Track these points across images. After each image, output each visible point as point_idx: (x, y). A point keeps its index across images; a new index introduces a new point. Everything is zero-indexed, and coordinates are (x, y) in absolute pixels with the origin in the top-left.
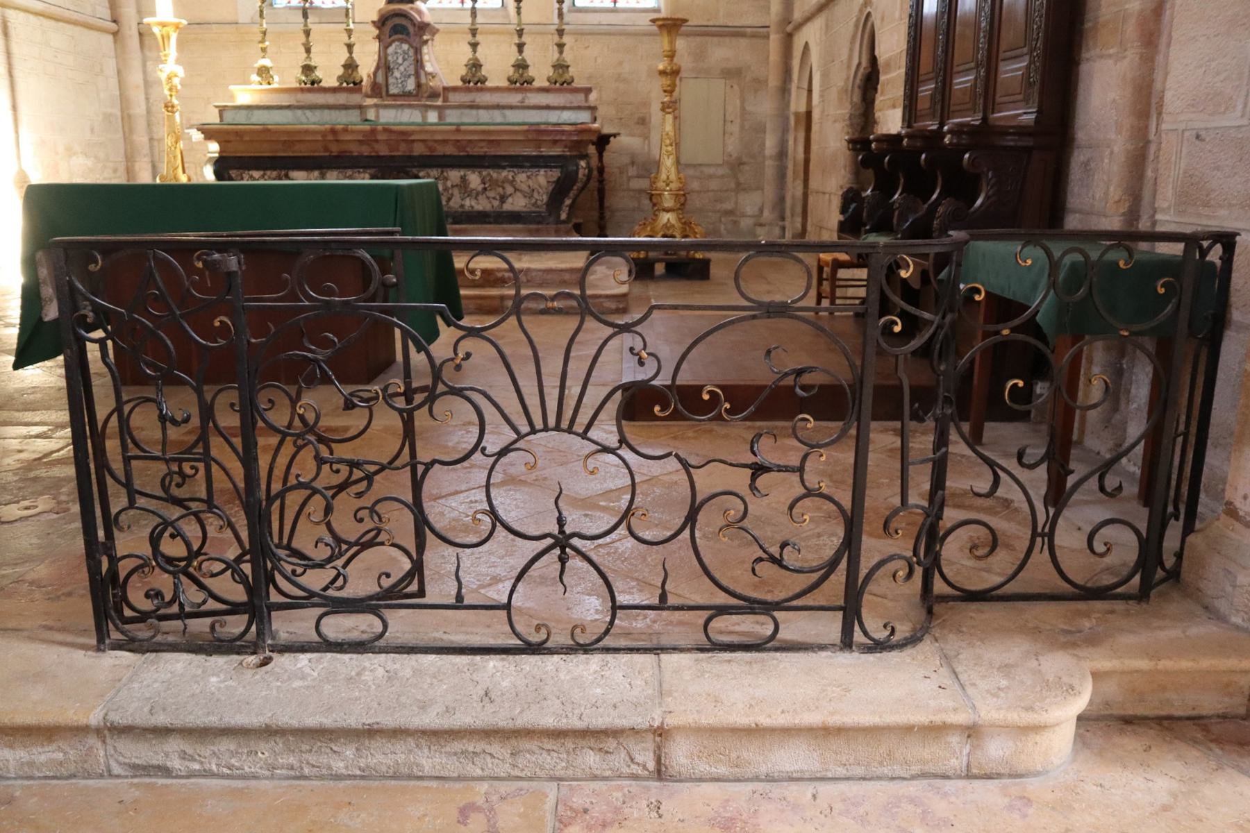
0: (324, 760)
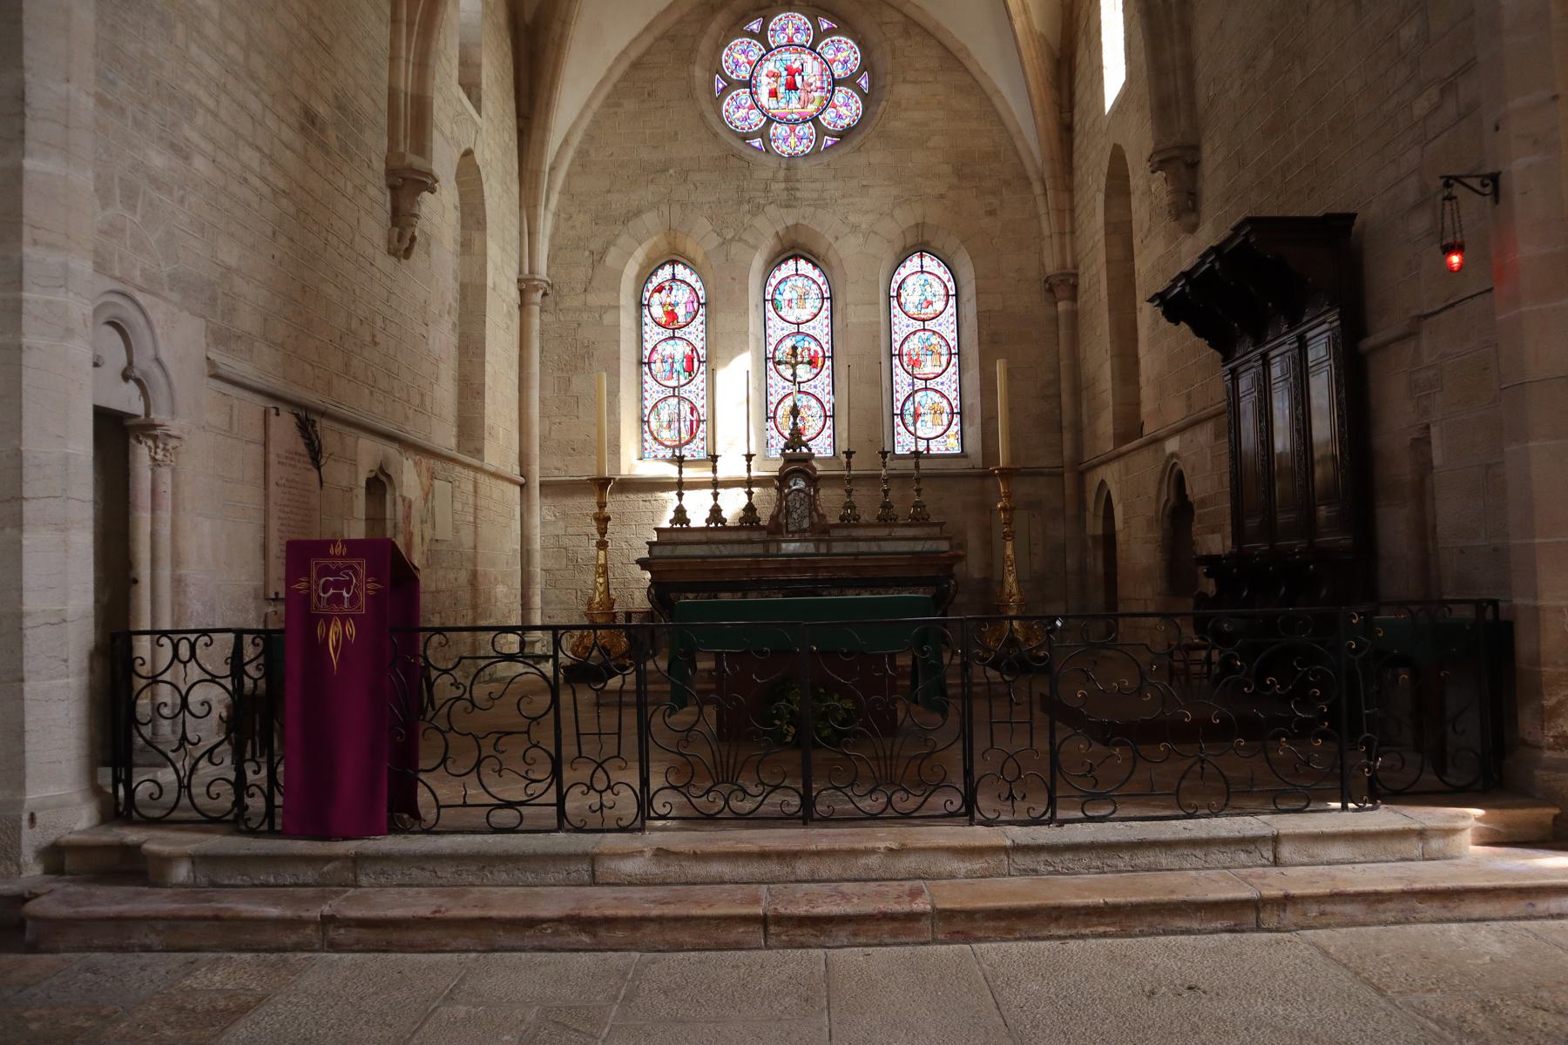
0: (1114, 862)
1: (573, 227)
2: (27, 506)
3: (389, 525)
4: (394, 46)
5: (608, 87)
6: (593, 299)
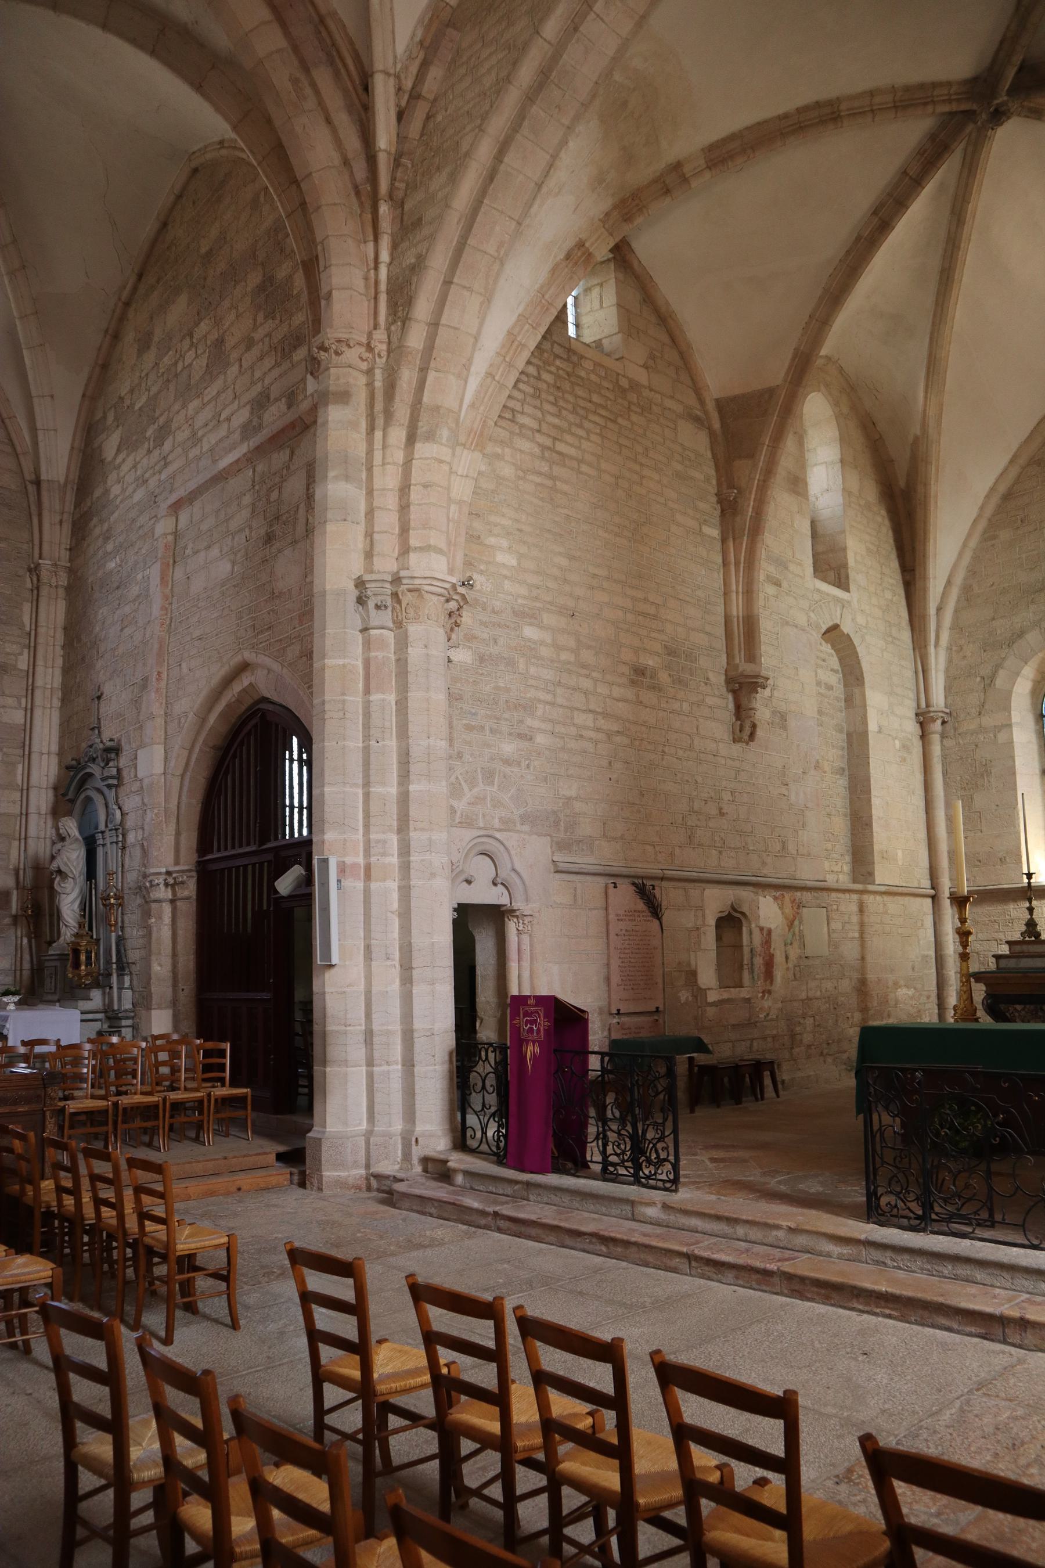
0: (940, 1268)
1: (965, 657)
2: (414, 972)
3: (746, 950)
4: (726, 583)
5: (982, 524)
6: (987, 721)
